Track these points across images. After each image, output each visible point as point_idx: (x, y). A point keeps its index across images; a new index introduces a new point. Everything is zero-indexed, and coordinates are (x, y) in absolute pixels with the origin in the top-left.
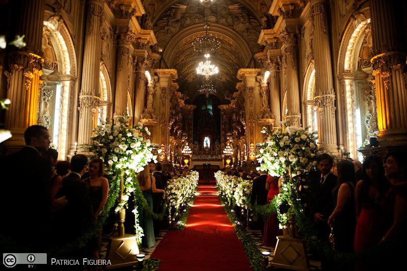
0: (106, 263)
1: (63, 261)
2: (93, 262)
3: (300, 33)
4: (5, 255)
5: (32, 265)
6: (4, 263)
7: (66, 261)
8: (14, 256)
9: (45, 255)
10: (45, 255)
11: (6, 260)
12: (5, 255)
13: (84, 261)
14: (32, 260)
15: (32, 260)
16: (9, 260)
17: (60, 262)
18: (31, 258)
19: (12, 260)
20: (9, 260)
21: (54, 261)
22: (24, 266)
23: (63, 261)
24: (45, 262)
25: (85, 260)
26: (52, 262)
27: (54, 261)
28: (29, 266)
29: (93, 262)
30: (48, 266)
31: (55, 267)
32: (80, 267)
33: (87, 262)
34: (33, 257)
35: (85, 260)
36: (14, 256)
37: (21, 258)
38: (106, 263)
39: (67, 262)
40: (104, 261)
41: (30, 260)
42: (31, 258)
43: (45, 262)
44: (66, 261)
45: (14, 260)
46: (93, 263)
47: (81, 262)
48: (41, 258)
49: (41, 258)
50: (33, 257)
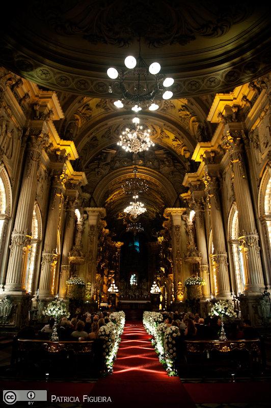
0: (107, 400)
1: (63, 399)
2: (93, 399)
4: (5, 392)
5: (32, 402)
6: (4, 400)
7: (66, 398)
8: (14, 393)
9: (45, 392)
10: (45, 392)
11: (6, 397)
12: (5, 392)
13: (84, 398)
14: (33, 397)
15: (33, 397)
16: (9, 397)
17: (60, 399)
18: (31, 395)
19: (12, 397)
20: (9, 397)
21: (54, 398)
22: (24, 403)
23: (63, 399)
24: (45, 399)
25: (85, 397)
26: (52, 399)
27: (54, 398)
28: (29, 403)
29: (93, 399)
30: (48, 403)
31: (56, 404)
32: (80, 404)
33: (87, 399)
34: (33, 394)
35: (85, 397)
36: (14, 393)
37: (21, 395)
38: (107, 400)
39: (67, 399)
40: (105, 398)
41: (30, 397)
42: (31, 395)
43: (45, 399)
44: (66, 398)
45: (14, 397)
46: (93, 400)
47: (81, 399)
48: (41, 395)
49: (41, 395)
50: (33, 394)
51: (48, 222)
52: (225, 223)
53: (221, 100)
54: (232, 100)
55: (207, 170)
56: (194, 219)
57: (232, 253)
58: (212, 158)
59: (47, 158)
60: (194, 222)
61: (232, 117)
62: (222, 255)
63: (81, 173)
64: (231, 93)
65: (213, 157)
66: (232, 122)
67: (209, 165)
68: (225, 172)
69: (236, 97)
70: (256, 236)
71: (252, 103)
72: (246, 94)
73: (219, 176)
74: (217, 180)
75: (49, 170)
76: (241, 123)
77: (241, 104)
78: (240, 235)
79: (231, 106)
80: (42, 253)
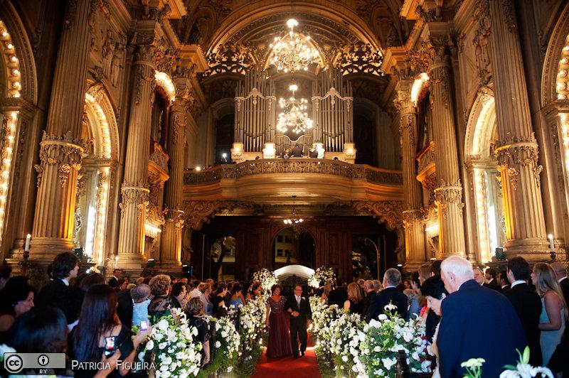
52: (461, 135)
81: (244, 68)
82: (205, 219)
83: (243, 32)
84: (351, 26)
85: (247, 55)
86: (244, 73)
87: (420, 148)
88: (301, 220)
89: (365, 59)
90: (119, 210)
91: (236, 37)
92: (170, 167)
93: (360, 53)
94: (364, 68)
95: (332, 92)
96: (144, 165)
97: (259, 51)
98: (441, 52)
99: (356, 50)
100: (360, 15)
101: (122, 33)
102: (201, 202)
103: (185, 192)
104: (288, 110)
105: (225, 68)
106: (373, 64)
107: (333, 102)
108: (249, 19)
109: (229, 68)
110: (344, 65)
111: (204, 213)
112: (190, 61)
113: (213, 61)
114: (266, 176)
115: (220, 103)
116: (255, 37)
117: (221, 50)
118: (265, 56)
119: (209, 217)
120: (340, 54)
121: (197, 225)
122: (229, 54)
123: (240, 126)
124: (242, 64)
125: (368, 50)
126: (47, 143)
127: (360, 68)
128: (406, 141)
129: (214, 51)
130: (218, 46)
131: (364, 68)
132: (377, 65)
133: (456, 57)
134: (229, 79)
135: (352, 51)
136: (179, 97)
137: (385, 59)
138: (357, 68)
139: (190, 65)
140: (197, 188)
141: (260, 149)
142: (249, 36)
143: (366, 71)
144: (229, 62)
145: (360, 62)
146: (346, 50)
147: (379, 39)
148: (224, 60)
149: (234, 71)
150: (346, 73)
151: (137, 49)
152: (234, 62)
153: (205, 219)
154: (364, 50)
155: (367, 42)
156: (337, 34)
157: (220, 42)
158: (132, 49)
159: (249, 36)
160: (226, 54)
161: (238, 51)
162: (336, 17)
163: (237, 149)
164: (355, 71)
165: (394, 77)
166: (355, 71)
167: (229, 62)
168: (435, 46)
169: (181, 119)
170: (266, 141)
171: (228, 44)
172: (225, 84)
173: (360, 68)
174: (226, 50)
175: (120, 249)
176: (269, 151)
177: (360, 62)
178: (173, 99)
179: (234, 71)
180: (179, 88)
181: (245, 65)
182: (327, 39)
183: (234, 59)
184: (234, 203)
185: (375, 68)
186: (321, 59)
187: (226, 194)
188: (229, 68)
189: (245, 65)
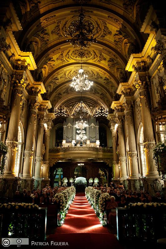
3: (150, 81)
51: (28, 132)
53: (134, 58)
54: (141, 58)
55: (125, 100)
56: (117, 129)
57: (140, 152)
58: (128, 93)
59: (27, 93)
60: (117, 131)
61: (140, 68)
62: (134, 152)
63: (47, 101)
64: (140, 53)
65: (129, 92)
66: (141, 71)
67: (127, 97)
68: (137, 102)
69: (143, 56)
70: (154, 143)
71: (153, 60)
72: (149, 55)
73: (132, 103)
74: (132, 106)
75: (28, 100)
76: (146, 72)
77: (146, 60)
78: (144, 142)
79: (140, 61)
80: (24, 151)
81: (65, 114)
82: (54, 164)
83: (65, 102)
84: (99, 101)
85: (66, 110)
86: (65, 116)
87: (117, 145)
88: (83, 164)
89: (103, 111)
90: (35, 163)
91: (63, 104)
92: (45, 149)
93: (101, 110)
94: (103, 114)
95: (93, 124)
96: (41, 151)
97: (70, 109)
98: (120, 120)
99: (100, 109)
100: (101, 99)
101: (26, 101)
102: (53, 158)
103: (49, 155)
104: (79, 134)
105: (59, 114)
106: (105, 113)
107: (93, 128)
108: (66, 99)
109: (61, 114)
110: (97, 114)
111: (54, 162)
112: (46, 106)
113: (56, 112)
114: (73, 152)
115: (58, 125)
116: (69, 104)
117: (58, 109)
118: (72, 110)
119: (55, 163)
120: (95, 110)
121: (52, 166)
122: (61, 110)
123: (64, 136)
124: (65, 113)
125: (104, 109)
126: (26, 152)
127: (102, 114)
128: (114, 140)
129: (56, 109)
130: (57, 107)
131: (103, 114)
132: (107, 113)
133: (124, 122)
134: (61, 118)
135: (99, 109)
136: (48, 128)
137: (108, 117)
138: (100, 114)
139: (46, 107)
140: (52, 154)
141: (71, 142)
142: (67, 104)
143: (103, 115)
144: (61, 112)
145: (101, 112)
146: (97, 109)
147: (107, 106)
148: (59, 112)
149: (62, 115)
150: (97, 116)
151: (40, 120)
152: (62, 112)
153: (54, 164)
154: (103, 109)
155: (104, 106)
156: (94, 103)
157: (58, 106)
158: (38, 119)
159: (67, 104)
160: (60, 110)
161: (63, 109)
162: (94, 98)
163: (64, 142)
164: (100, 115)
165: (111, 122)
166: (100, 115)
167: (61, 112)
168: (128, 104)
169: (48, 133)
170: (73, 139)
171: (61, 106)
172: (59, 119)
173: (102, 114)
174: (60, 109)
175: (35, 175)
176: (74, 142)
177: (101, 112)
178: (46, 129)
179: (62, 115)
180: (48, 125)
181: (66, 113)
182: (91, 105)
183: (62, 111)
184: (62, 159)
185: (106, 114)
186: (89, 111)
187: (61, 156)
188: (61, 114)
189: (66, 113)
